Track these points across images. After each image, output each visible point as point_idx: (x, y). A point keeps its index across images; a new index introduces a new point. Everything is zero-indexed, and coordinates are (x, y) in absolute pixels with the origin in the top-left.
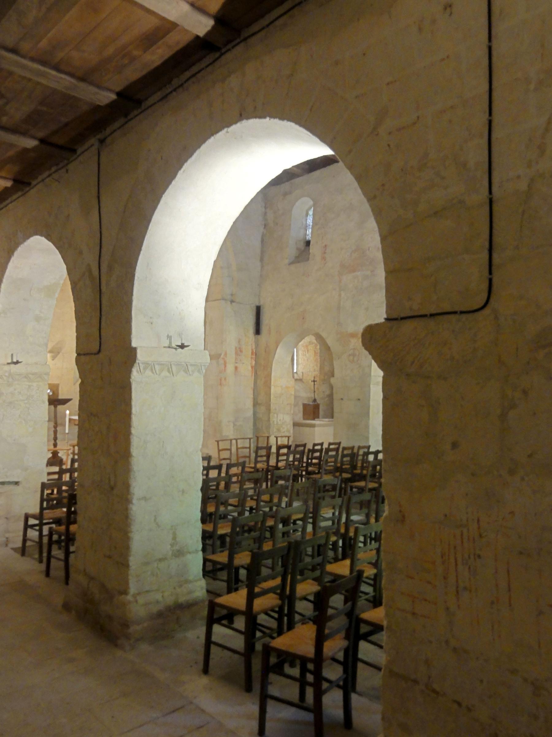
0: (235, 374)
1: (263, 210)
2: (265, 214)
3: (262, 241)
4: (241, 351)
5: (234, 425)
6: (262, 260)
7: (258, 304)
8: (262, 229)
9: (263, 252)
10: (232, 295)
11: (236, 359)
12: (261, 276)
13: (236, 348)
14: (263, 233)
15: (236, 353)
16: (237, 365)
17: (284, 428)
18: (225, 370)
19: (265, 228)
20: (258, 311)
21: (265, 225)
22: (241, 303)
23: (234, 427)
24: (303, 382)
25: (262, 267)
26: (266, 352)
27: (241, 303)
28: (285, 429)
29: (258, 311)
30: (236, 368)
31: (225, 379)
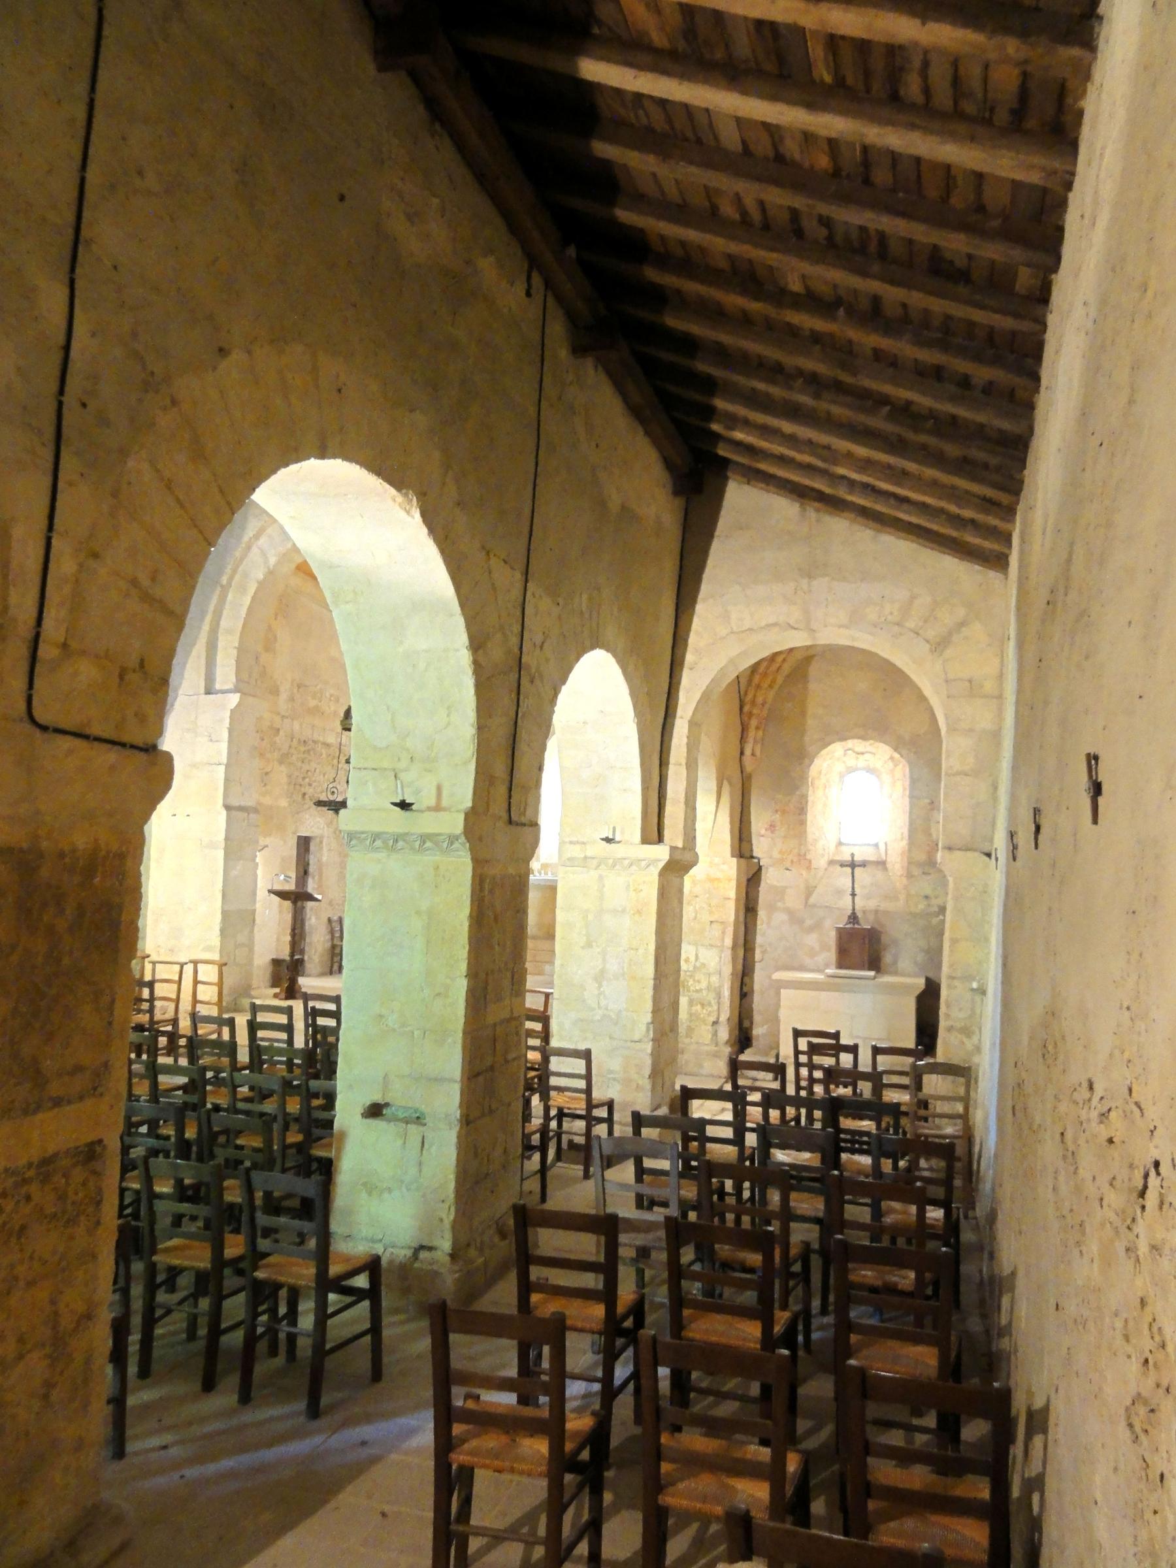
17: (699, 982)
24: (886, 869)
28: (704, 985)
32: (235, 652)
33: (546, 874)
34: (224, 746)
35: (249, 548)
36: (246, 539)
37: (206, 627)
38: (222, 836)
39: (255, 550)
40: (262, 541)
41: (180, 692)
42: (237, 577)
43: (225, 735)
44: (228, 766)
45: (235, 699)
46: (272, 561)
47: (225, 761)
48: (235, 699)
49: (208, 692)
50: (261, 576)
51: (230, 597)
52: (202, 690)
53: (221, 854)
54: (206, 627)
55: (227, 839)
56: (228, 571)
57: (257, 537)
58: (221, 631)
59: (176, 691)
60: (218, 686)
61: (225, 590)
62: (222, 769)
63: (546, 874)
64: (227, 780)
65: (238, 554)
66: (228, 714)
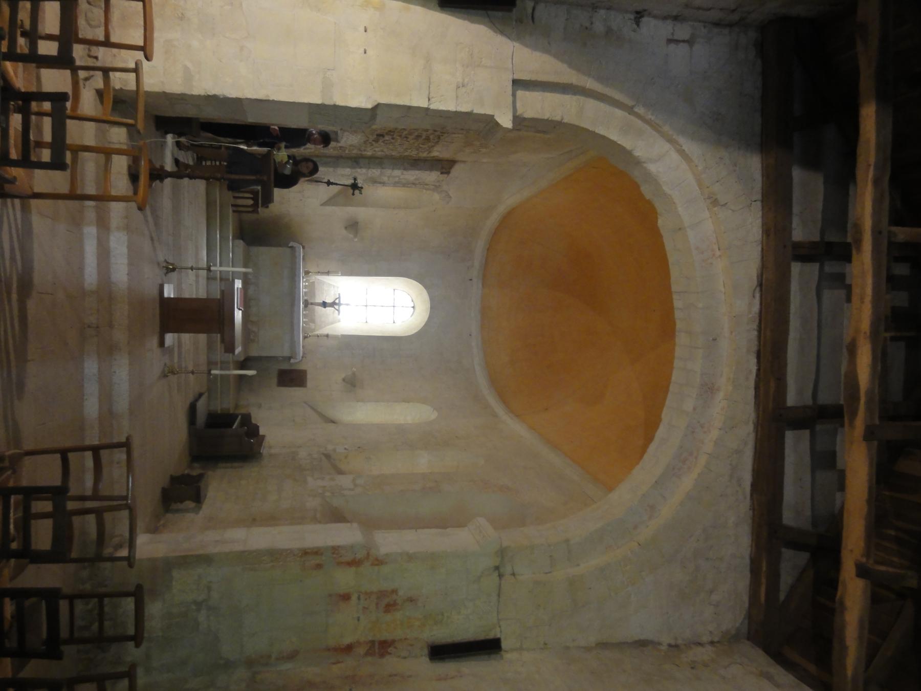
0: (330, 595)
1: (705, 639)
2: (700, 644)
3: (642, 644)
4: (390, 607)
5: (199, 605)
6: (603, 645)
7: (504, 645)
8: (666, 640)
9: (621, 645)
10: (513, 574)
11: (368, 594)
12: (568, 648)
13: (394, 591)
14: (660, 644)
15: (382, 594)
16: (354, 598)
18: (340, 564)
19: (670, 645)
20: (488, 647)
21: (677, 646)
22: (499, 596)
23: (195, 602)
25: (588, 649)
26: (390, 676)
27: (499, 596)
29: (488, 647)
30: (346, 597)
31: (319, 566)
32: (558, 118)
33: (305, 287)
34: (451, 106)
35: (670, 141)
36: (681, 140)
37: (590, 83)
38: (340, 100)
39: (667, 146)
40: (675, 156)
41: (517, 44)
42: (639, 123)
43: (464, 108)
44: (427, 109)
45: (506, 121)
46: (652, 168)
47: (432, 107)
48: (506, 121)
49: (517, 83)
50: (637, 153)
51: (619, 113)
52: (516, 77)
53: (315, 99)
54: (590, 83)
55: (335, 107)
56: (649, 116)
57: (681, 152)
58: (582, 98)
59: (518, 38)
60: (520, 93)
61: (630, 110)
62: (424, 104)
63: (305, 287)
64: (409, 108)
65: (666, 128)
66: (489, 112)
